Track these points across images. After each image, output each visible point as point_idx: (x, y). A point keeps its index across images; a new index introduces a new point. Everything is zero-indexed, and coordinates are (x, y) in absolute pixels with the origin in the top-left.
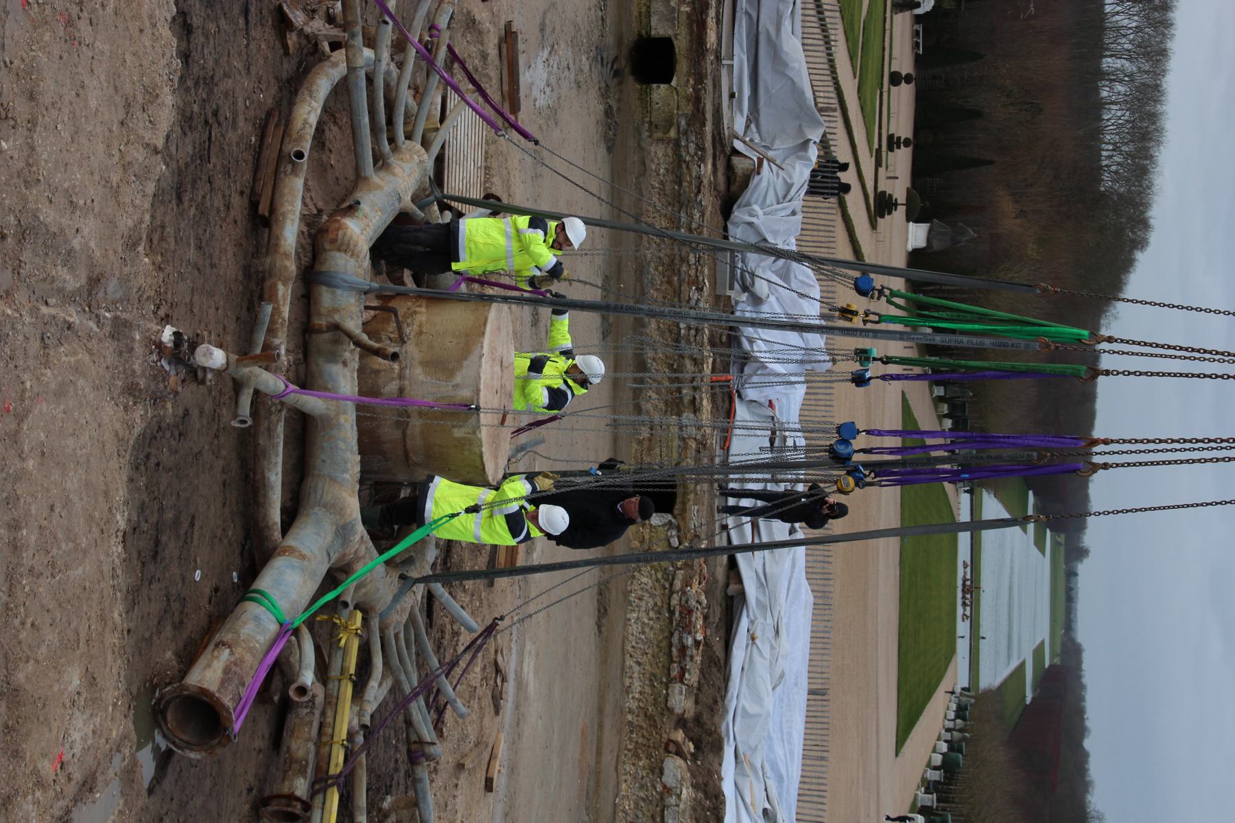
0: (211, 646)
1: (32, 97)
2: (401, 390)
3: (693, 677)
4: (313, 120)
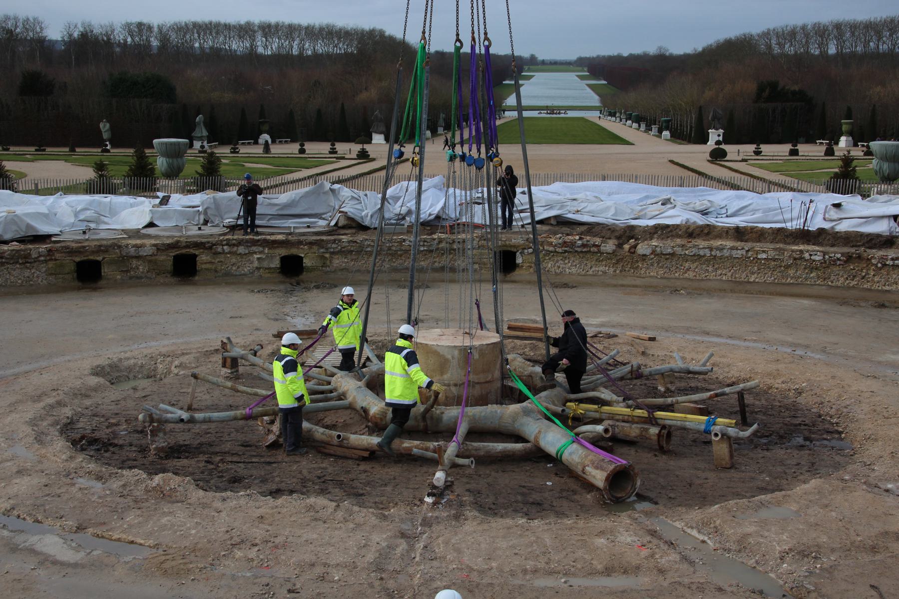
0: (585, 476)
1: (313, 565)
2: (456, 385)
3: (598, 241)
4: (321, 430)
